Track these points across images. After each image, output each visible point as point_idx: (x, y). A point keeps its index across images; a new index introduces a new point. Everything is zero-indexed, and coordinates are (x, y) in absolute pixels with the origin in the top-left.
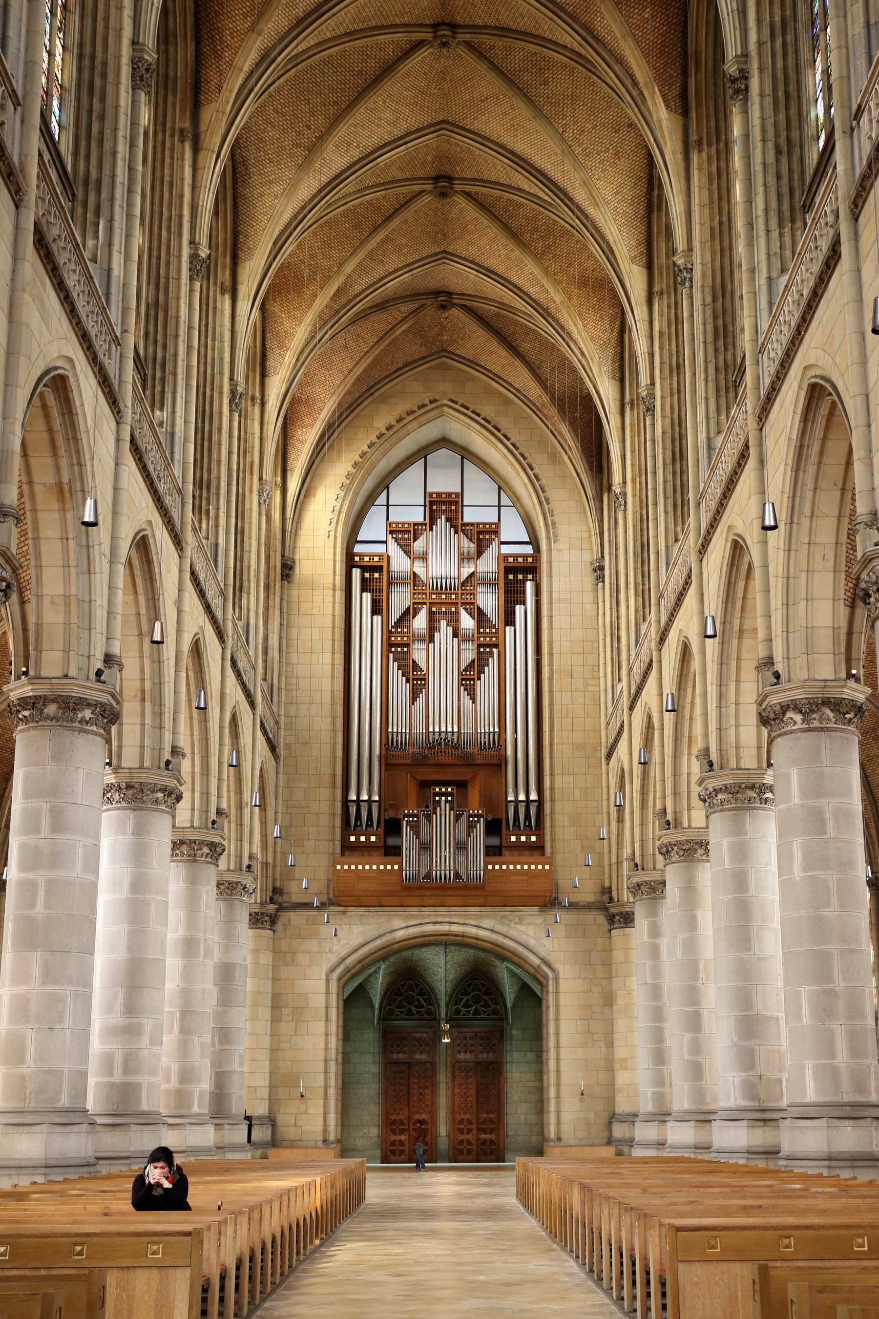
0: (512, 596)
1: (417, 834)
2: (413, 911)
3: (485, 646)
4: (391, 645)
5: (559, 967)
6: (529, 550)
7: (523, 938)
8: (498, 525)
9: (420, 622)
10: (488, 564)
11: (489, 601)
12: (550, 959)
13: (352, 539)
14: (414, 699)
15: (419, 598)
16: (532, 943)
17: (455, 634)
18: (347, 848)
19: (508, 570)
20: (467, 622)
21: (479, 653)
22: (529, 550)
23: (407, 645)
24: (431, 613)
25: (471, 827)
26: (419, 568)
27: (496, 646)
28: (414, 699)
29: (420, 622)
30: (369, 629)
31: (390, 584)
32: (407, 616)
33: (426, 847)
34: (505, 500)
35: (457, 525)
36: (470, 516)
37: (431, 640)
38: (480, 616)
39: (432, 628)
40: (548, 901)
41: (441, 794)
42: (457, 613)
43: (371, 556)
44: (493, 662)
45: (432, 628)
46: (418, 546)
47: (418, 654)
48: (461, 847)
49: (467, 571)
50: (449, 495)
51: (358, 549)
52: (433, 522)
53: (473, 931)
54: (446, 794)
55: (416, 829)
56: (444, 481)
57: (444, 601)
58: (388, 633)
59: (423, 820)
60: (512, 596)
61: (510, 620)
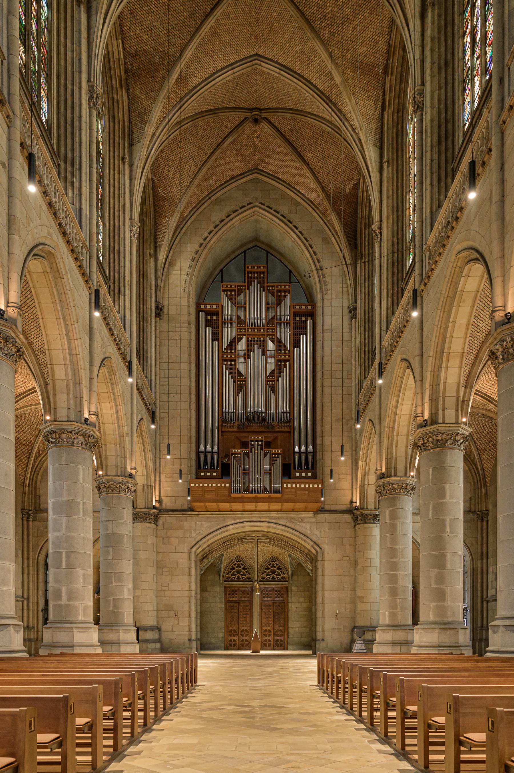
0: (299, 330)
1: (240, 464)
3: (281, 361)
9: (242, 346)
11: (284, 334)
15: (241, 332)
17: (263, 354)
19: (296, 315)
20: (270, 346)
23: (234, 361)
26: (242, 314)
27: (288, 361)
29: (242, 346)
30: (211, 351)
31: (223, 323)
32: (233, 343)
33: (246, 473)
37: (249, 357)
38: (279, 343)
39: (249, 349)
42: (264, 341)
44: (287, 371)
45: (249, 349)
47: (241, 366)
48: (267, 473)
49: (270, 314)
52: (249, 284)
55: (239, 461)
58: (222, 352)
59: (244, 456)
60: (299, 330)
61: (297, 345)
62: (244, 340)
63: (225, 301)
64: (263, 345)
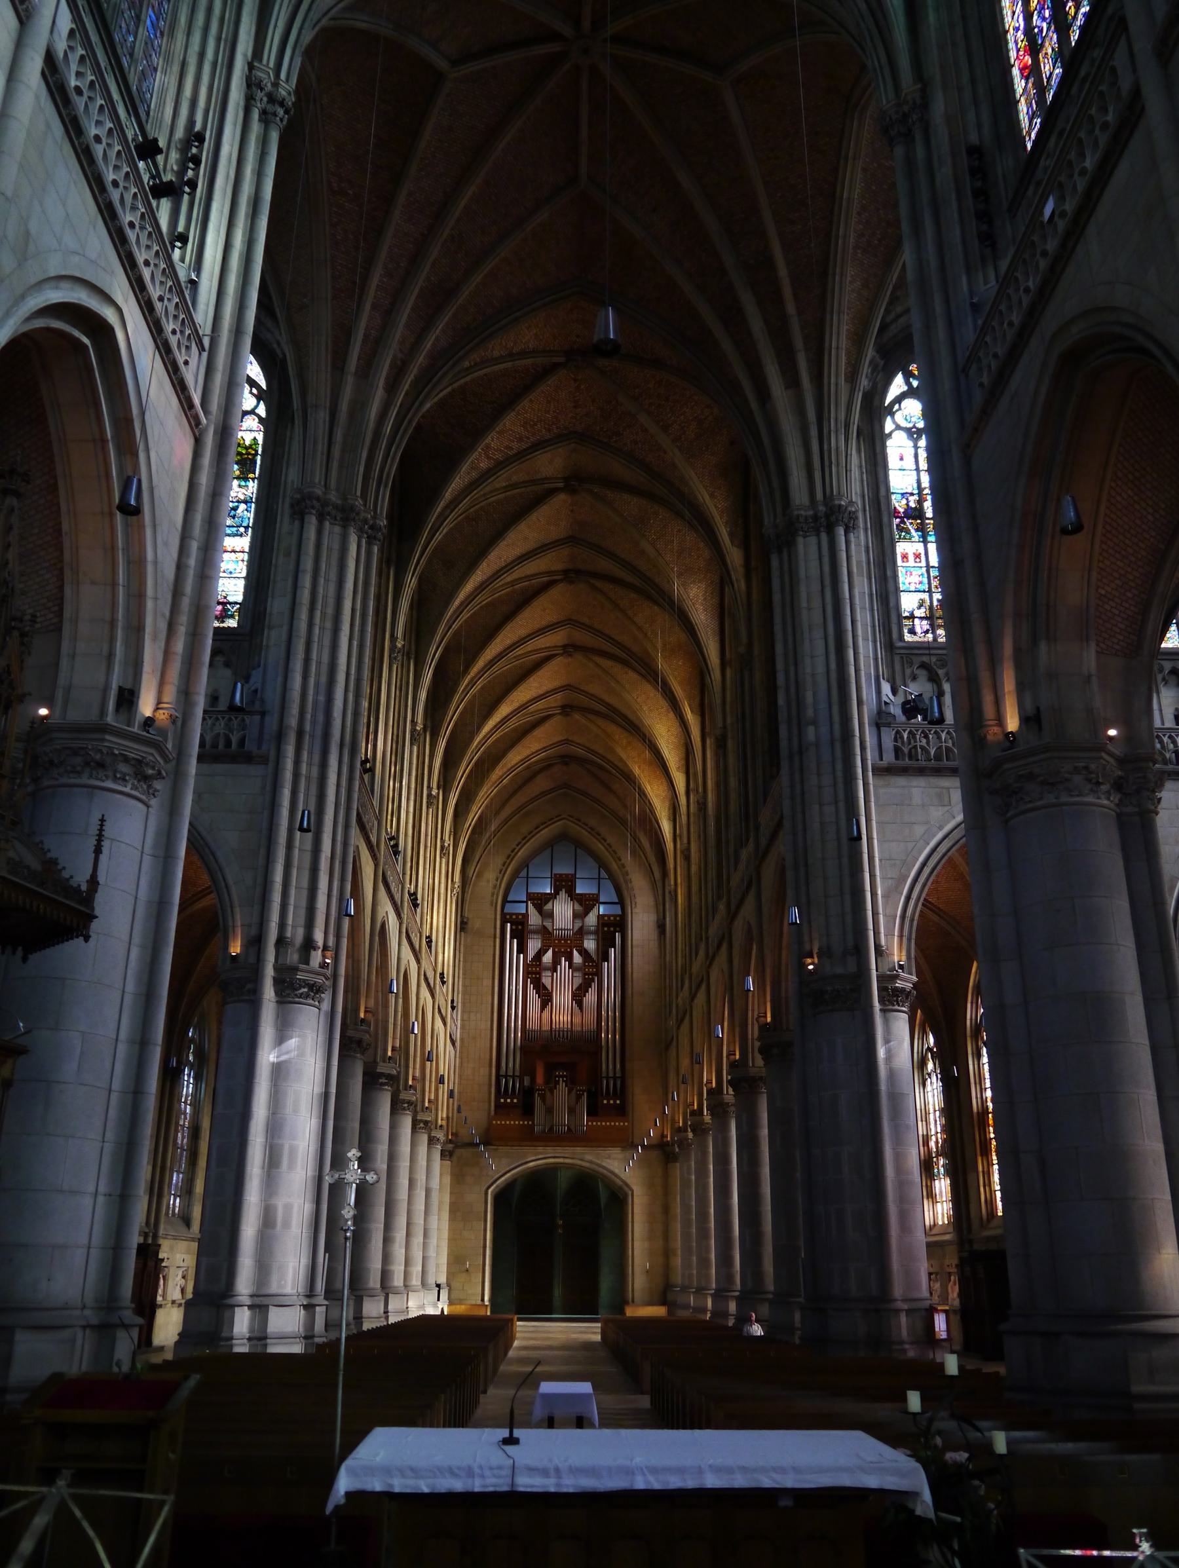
0: (606, 942)
2: (541, 1149)
4: (529, 973)
5: (635, 1188)
6: (617, 910)
7: (611, 1168)
8: (598, 895)
9: (548, 957)
10: (591, 920)
11: (590, 944)
12: (629, 1181)
13: (505, 901)
14: (543, 1009)
16: (617, 1171)
18: (498, 1106)
20: (577, 958)
21: (584, 979)
22: (617, 910)
23: (540, 974)
24: (554, 952)
25: (579, 1097)
26: (548, 924)
28: (543, 1009)
29: (548, 957)
30: (515, 965)
34: (604, 874)
35: (572, 895)
36: (579, 890)
39: (556, 962)
40: (627, 1142)
41: (559, 1076)
42: (571, 953)
43: (517, 915)
45: (556, 962)
46: (548, 907)
47: (546, 980)
49: (578, 924)
50: (567, 875)
51: (509, 908)
53: (579, 1162)
54: (563, 1076)
56: (564, 869)
57: (563, 946)
60: (606, 942)
61: (606, 958)
62: (550, 953)
63: (532, 910)
64: (570, 958)
